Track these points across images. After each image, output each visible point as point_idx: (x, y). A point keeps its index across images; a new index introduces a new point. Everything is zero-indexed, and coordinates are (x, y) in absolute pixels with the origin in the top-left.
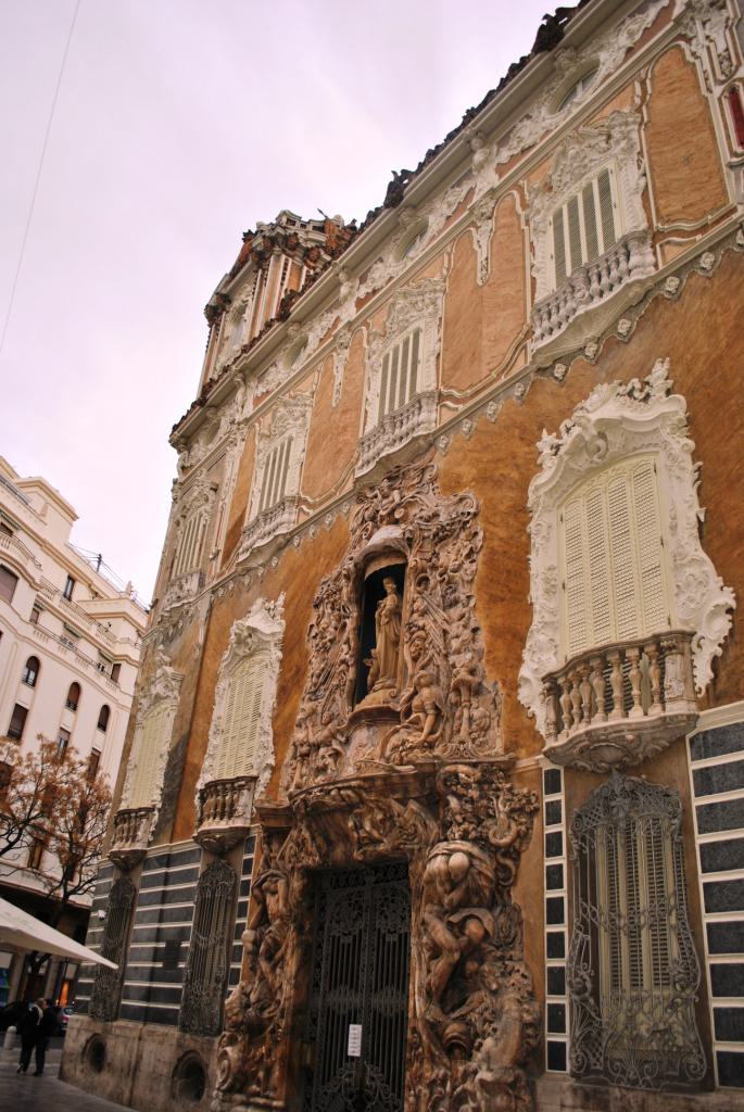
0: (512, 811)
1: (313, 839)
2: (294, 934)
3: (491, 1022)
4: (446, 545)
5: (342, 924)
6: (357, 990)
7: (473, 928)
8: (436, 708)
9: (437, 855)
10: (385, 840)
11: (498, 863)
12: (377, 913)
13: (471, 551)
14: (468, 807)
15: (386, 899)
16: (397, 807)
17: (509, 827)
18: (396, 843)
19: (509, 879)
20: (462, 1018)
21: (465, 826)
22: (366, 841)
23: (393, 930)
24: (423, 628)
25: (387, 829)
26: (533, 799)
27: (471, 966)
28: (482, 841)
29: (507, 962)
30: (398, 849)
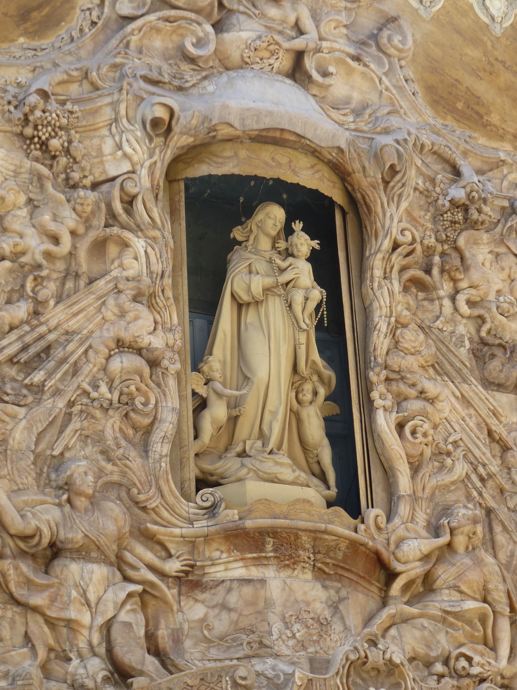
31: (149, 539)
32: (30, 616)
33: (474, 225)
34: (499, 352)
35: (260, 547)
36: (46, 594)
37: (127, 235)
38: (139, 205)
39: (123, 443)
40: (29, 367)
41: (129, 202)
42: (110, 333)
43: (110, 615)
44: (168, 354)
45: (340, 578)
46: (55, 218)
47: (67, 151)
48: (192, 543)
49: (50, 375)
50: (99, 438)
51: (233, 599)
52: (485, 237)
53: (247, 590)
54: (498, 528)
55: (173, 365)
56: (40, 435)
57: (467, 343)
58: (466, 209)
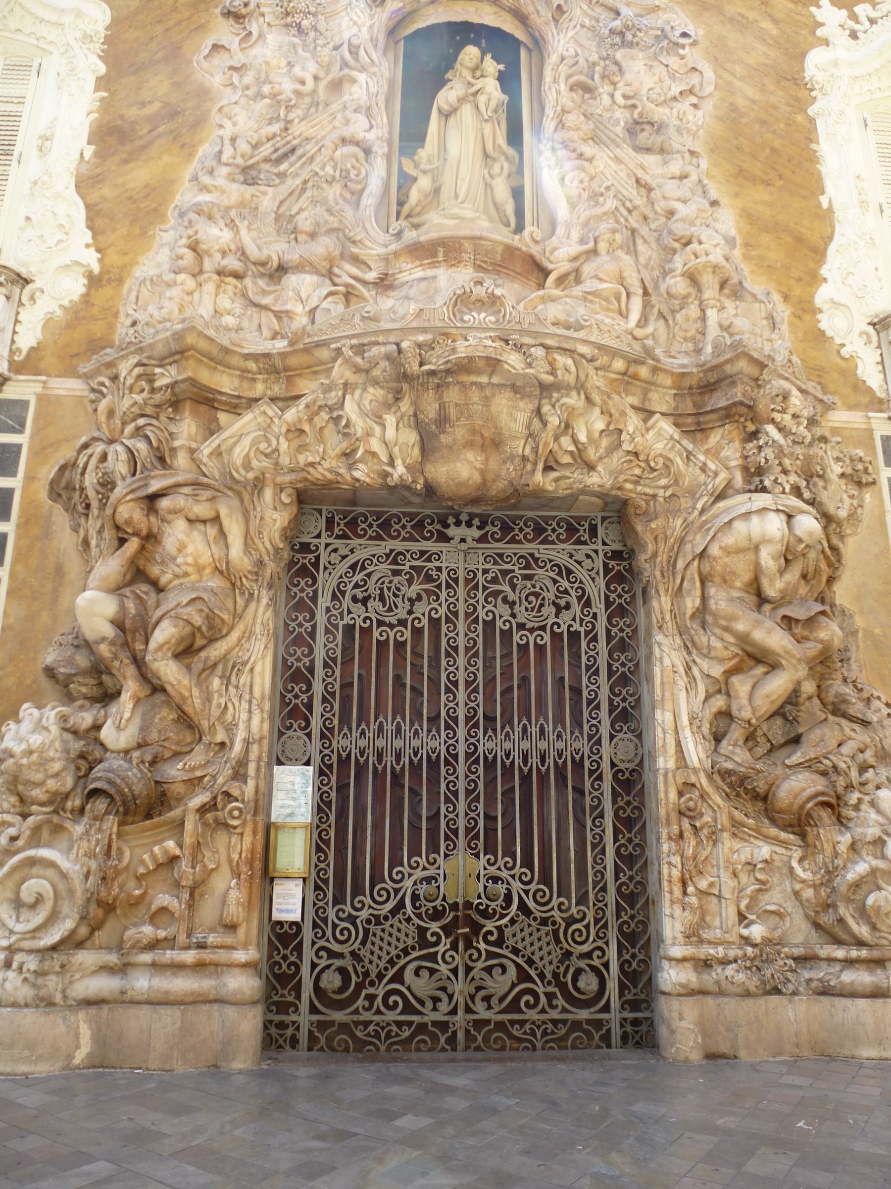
0: (843, 475)
2: (269, 613)
4: (632, 58)
8: (646, 293)
10: (599, 468)
12: (481, 596)
13: (691, 92)
14: (799, 450)
15: (504, 573)
16: (633, 422)
18: (622, 478)
22: (567, 459)
24: (590, 160)
25: (602, 451)
26: (871, 470)
30: (620, 488)
31: (356, 260)
32: (263, 313)
33: (631, 45)
34: (648, 127)
35: (434, 255)
36: (272, 297)
37: (355, 74)
38: (362, 52)
39: (341, 201)
40: (278, 161)
41: (354, 51)
42: (336, 134)
43: (314, 305)
44: (378, 143)
45: (498, 273)
46: (304, 69)
47: (316, 30)
48: (386, 260)
49: (292, 165)
50: (324, 202)
51: (413, 292)
52: (641, 55)
53: (423, 285)
54: (639, 242)
55: (380, 149)
56: (282, 203)
57: (622, 124)
58: (622, 34)
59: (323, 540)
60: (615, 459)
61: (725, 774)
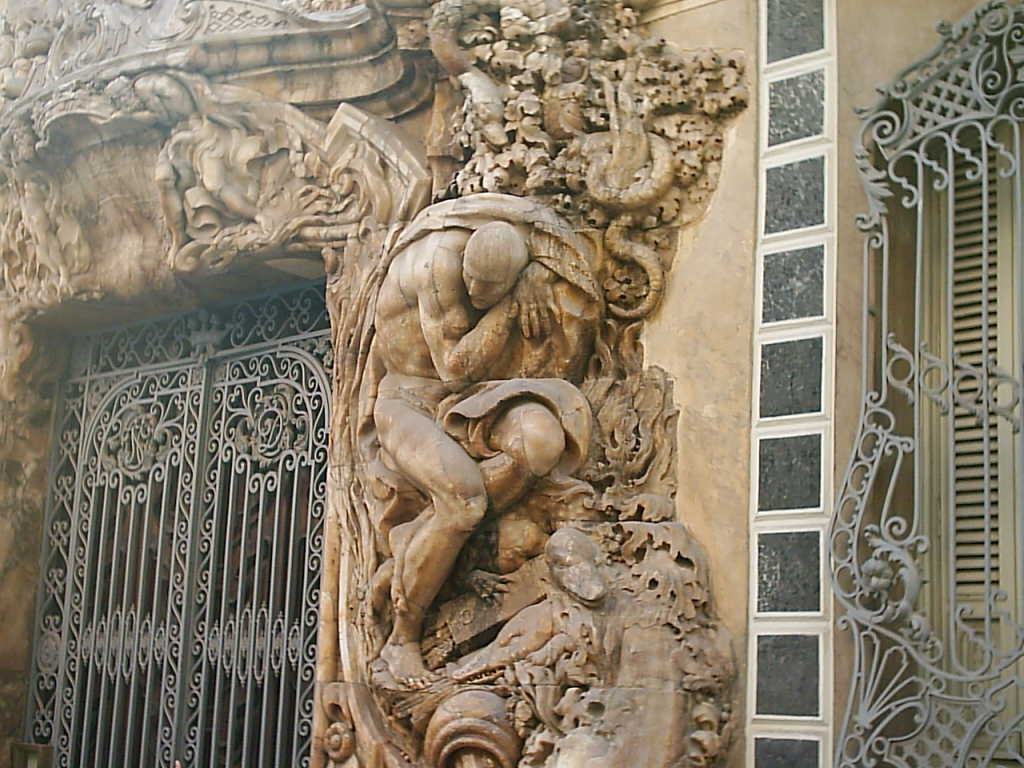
0: (664, 110)
1: (52, 229)
3: (585, 687)
5: (124, 457)
6: (162, 618)
7: (529, 431)
9: (426, 233)
11: (608, 250)
14: (528, 100)
15: (249, 387)
17: (650, 158)
19: (639, 299)
20: (488, 677)
21: (518, 152)
22: (205, 219)
23: (264, 462)
26: (729, 77)
27: (517, 533)
28: (563, 191)
29: (628, 526)
59: (89, 378)
60: (287, 195)
61: (379, 690)
